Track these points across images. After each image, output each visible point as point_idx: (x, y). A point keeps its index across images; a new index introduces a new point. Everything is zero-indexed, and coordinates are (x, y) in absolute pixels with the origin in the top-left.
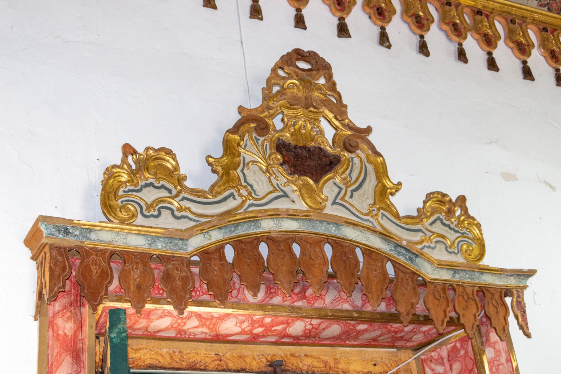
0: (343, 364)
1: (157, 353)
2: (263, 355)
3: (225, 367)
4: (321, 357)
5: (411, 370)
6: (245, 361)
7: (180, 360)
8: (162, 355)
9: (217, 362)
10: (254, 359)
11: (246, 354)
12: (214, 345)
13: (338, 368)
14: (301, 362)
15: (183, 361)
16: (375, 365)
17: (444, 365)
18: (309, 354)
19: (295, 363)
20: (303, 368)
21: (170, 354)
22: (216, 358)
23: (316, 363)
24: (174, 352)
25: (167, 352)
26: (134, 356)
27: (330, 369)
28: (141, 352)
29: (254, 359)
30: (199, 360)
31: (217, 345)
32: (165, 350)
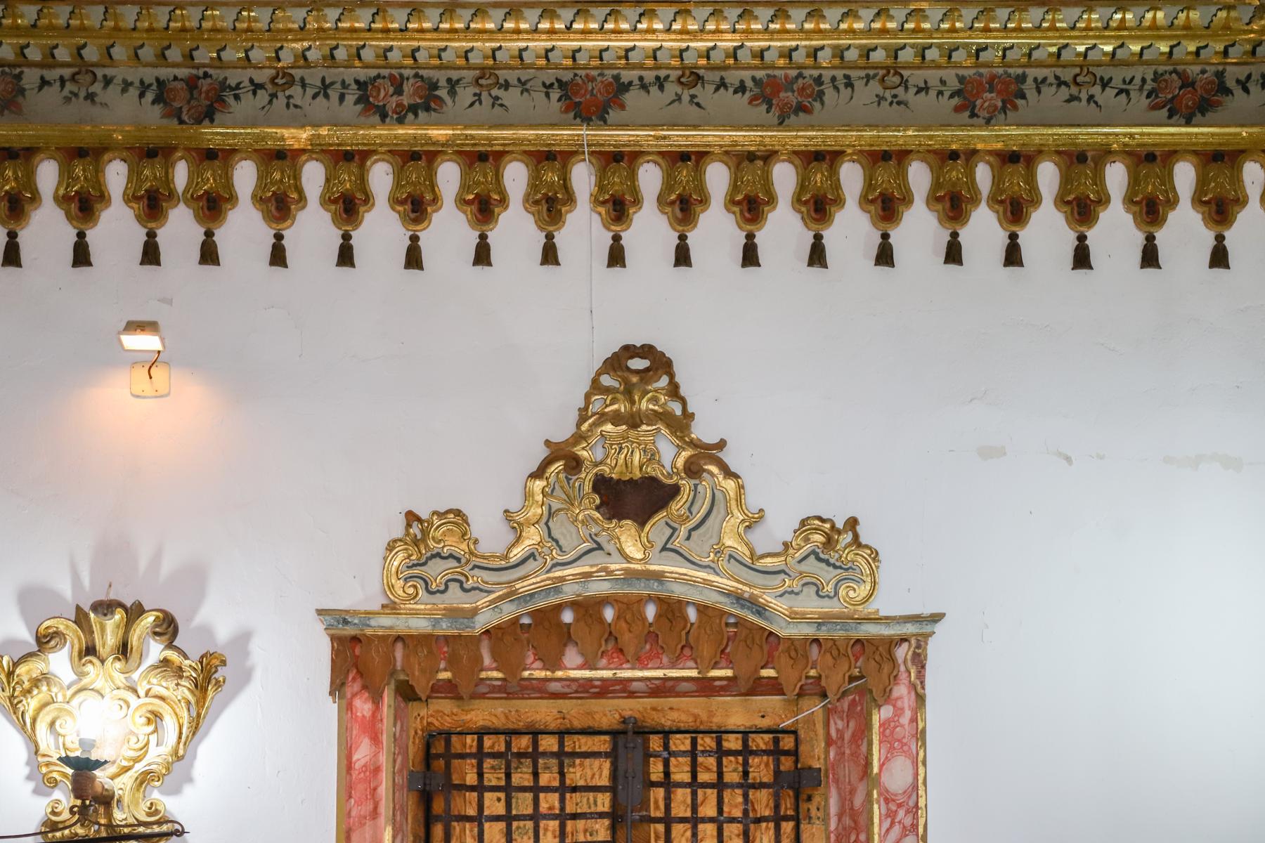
0: (719, 718)
1: (490, 714)
2: (617, 710)
3: (569, 726)
4: (691, 710)
5: (814, 721)
6: (593, 718)
7: (517, 720)
8: (496, 716)
9: (559, 721)
10: (605, 715)
11: (595, 710)
12: (558, 701)
13: (711, 722)
14: (664, 717)
15: (520, 721)
16: (763, 717)
17: (843, 720)
18: (675, 707)
19: (656, 717)
20: (666, 724)
21: (505, 714)
22: (558, 716)
23: (684, 717)
24: (510, 711)
25: (502, 712)
26: (465, 718)
27: (701, 723)
28: (473, 713)
29: (605, 715)
30: (538, 719)
31: (561, 701)
32: (500, 710)
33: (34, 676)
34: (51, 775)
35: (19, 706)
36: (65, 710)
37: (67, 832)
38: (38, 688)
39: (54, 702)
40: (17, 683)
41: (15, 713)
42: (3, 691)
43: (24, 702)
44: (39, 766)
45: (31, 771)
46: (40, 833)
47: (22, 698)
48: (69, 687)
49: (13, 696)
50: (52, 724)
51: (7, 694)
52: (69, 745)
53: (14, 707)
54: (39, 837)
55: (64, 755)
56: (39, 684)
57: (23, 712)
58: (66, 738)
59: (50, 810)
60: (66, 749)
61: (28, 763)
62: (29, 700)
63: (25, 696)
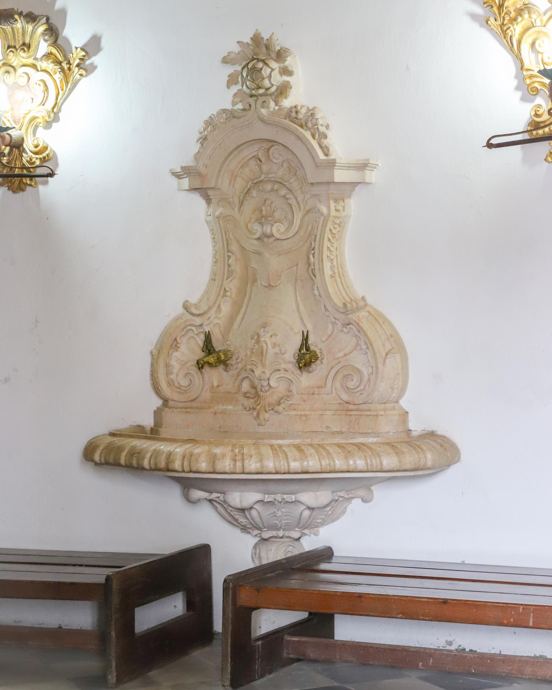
33: (519, 6)
34: (533, 85)
35: (508, 31)
36: (543, 32)
37: (547, 129)
38: (521, 16)
39: (534, 27)
40: (506, 13)
41: (505, 37)
42: (496, 20)
43: (512, 28)
44: (524, 79)
45: (519, 83)
46: (527, 131)
47: (510, 25)
48: (545, 14)
49: (503, 24)
50: (533, 44)
51: (499, 22)
52: (546, 60)
53: (504, 32)
54: (526, 134)
55: (543, 68)
56: (523, 13)
57: (511, 37)
58: (544, 54)
59: (533, 113)
60: (544, 64)
61: (516, 77)
62: (515, 26)
63: (512, 23)
